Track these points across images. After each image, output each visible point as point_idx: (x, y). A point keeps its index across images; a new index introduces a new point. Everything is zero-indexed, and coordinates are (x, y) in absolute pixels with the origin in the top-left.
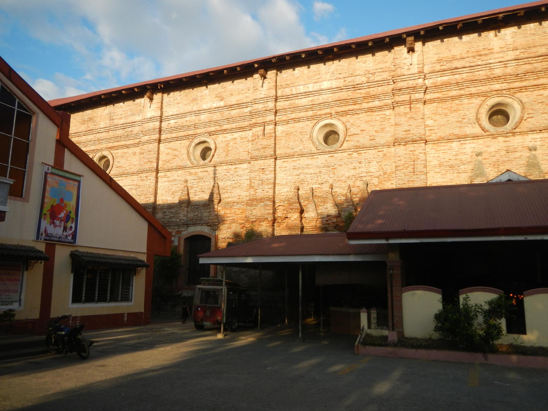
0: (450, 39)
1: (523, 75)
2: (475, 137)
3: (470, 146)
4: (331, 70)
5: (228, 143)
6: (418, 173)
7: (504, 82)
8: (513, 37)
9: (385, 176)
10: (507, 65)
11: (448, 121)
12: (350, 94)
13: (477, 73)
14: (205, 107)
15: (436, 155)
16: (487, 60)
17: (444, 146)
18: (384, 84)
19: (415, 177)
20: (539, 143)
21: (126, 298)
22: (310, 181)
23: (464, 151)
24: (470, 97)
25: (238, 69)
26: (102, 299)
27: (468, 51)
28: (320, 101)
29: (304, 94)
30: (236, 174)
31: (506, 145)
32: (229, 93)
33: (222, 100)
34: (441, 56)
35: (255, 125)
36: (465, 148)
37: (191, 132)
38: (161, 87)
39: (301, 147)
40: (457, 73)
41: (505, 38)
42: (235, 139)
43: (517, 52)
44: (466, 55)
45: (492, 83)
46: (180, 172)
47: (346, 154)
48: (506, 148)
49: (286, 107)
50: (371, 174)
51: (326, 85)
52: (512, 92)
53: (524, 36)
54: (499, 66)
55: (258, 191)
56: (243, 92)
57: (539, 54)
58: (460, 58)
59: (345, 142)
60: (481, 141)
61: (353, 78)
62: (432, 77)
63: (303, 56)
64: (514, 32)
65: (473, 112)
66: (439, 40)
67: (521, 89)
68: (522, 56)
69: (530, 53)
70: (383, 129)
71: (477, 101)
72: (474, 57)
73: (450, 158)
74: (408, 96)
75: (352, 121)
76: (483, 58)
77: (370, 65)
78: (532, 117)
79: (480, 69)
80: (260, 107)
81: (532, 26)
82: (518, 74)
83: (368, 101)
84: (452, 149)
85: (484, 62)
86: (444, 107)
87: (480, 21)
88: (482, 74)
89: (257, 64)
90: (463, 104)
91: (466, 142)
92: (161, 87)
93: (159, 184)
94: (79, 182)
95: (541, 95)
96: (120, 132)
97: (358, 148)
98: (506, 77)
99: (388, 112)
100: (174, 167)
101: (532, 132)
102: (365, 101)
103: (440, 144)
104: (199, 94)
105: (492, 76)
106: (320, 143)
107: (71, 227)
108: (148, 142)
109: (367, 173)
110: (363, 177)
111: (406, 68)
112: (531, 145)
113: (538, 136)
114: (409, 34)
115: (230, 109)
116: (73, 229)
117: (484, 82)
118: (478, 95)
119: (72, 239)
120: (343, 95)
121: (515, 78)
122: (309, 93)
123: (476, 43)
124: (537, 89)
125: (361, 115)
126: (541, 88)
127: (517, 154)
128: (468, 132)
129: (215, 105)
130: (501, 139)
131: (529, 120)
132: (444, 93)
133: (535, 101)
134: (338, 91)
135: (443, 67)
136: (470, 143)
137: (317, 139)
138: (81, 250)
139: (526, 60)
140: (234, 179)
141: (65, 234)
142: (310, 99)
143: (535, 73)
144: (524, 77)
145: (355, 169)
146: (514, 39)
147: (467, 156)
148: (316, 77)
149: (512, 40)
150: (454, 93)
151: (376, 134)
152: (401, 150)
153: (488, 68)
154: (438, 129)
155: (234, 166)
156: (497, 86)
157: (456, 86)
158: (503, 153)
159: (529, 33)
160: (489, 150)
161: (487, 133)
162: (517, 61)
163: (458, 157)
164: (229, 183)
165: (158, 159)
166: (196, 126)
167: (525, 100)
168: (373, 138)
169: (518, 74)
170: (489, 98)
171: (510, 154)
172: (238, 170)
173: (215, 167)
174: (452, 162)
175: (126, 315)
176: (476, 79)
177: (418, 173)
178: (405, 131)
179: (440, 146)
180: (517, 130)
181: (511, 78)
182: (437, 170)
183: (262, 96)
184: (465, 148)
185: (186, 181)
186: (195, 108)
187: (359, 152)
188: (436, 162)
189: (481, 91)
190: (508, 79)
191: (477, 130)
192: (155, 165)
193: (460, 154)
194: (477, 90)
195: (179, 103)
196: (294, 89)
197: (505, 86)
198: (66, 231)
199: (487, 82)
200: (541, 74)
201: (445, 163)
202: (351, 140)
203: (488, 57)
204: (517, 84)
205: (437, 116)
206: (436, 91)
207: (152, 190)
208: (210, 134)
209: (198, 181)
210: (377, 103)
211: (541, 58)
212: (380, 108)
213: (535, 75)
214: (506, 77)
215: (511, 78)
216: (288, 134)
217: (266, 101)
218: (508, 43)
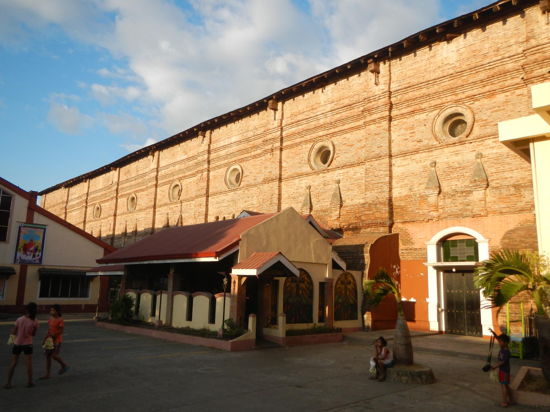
0: (298, 98)
1: (334, 123)
2: (307, 174)
3: (305, 181)
4: (237, 128)
5: (187, 185)
6: (274, 204)
7: (325, 129)
8: (332, 92)
9: (261, 207)
10: (327, 116)
11: (294, 162)
12: (245, 146)
13: (311, 123)
14: (178, 159)
15: (287, 190)
16: (316, 113)
17: (291, 182)
18: (262, 137)
19: (271, 207)
20: (341, 177)
21: (85, 294)
22: (224, 212)
23: (301, 185)
24: (306, 143)
25: (187, 133)
26: (65, 295)
27: (307, 107)
28: (231, 152)
29: (223, 147)
30: (190, 208)
31: (324, 180)
32: (189, 149)
33: (186, 154)
34: (293, 111)
35: (197, 172)
36: (302, 184)
37: (171, 179)
38: (154, 148)
39: (221, 187)
40: (300, 124)
41: (328, 93)
42: (191, 182)
43: (333, 104)
44: (305, 110)
45: (318, 131)
46: (165, 207)
47: (242, 191)
48: (323, 182)
49: (214, 158)
50: (254, 206)
51: (234, 139)
52: (329, 137)
53: (338, 91)
54: (322, 117)
55: (198, 220)
56: (196, 147)
57: (345, 105)
58: (303, 112)
59: (242, 182)
60: (310, 177)
61: (247, 133)
62: (286, 129)
63: (216, 121)
64: (333, 88)
65: (307, 154)
66: (300, 95)
67: (334, 134)
68: (336, 107)
69: (340, 105)
70: (261, 171)
71: (309, 146)
72: (309, 111)
73: (294, 191)
74: (272, 145)
75: (246, 166)
76: (314, 111)
77: (256, 122)
78: (339, 157)
79: (312, 121)
80: (200, 158)
81: (343, 82)
82: (332, 123)
83: (254, 150)
84: (295, 185)
85: (314, 115)
86: (293, 151)
87: (303, 85)
88: (313, 124)
89: (195, 128)
90: (302, 149)
91: (303, 178)
92: (154, 148)
93: (156, 216)
94: (45, 229)
95: (345, 138)
96: (140, 180)
97: (249, 186)
98: (325, 125)
99: (263, 158)
100: (163, 204)
101: (338, 169)
102: (253, 150)
103: (289, 181)
104: (176, 151)
105: (319, 125)
106: (231, 183)
107: (38, 255)
108: (151, 187)
109: (252, 205)
110: (249, 208)
111: (272, 123)
112: (337, 178)
113: (341, 171)
114: (269, 98)
115: (189, 161)
116: (40, 256)
117: (313, 131)
118: (310, 141)
119: (39, 261)
120: (242, 146)
121: (331, 126)
122: (225, 146)
123: (312, 99)
124: (343, 133)
125: (250, 161)
126: (345, 133)
127: (330, 186)
128: (304, 171)
129: (183, 158)
130: (321, 175)
131: (337, 158)
132: (293, 141)
133: (341, 143)
134: (239, 144)
135: (293, 121)
136: (304, 179)
137: (229, 181)
138: (46, 267)
139: (337, 111)
140: (189, 212)
141: (34, 259)
142: (226, 150)
143: (341, 121)
144: (335, 124)
145: (246, 202)
146: (332, 93)
147: (303, 189)
148: (230, 134)
149: (331, 95)
150: (298, 140)
151: (258, 175)
152: (266, 187)
153: (316, 119)
154: (288, 169)
155: (190, 202)
156: (321, 133)
157: (299, 135)
158: (322, 186)
159: (341, 88)
160: (314, 184)
161: (314, 171)
162: (332, 112)
163: (298, 191)
164: (187, 214)
165: (155, 199)
166: (173, 174)
167: (336, 143)
168: (255, 178)
169: (332, 123)
170: (316, 143)
171: (326, 186)
172: (191, 205)
173: (181, 203)
174: (295, 195)
175: (83, 306)
176: (308, 128)
177: (274, 204)
178: (269, 173)
179: (289, 183)
180: (330, 167)
181: (328, 126)
182: (287, 201)
183: (202, 150)
184: (302, 184)
185: (168, 214)
186: (174, 161)
187: (248, 189)
188: (286, 195)
189: (312, 138)
190: (326, 127)
191: (307, 169)
192: (153, 203)
193: (299, 188)
194: (310, 137)
195: (166, 158)
196: (218, 144)
197: (326, 132)
198: (35, 257)
199: (315, 130)
200: (344, 122)
201: (291, 196)
202: (245, 180)
203: (317, 110)
204: (332, 131)
205: (288, 159)
206: (288, 140)
207: (151, 221)
208: (180, 179)
209: (173, 214)
210: (259, 151)
211: (345, 108)
212: (260, 155)
213: (341, 123)
214: (325, 125)
215: (328, 126)
216: (215, 177)
217: (203, 154)
218: (329, 97)
